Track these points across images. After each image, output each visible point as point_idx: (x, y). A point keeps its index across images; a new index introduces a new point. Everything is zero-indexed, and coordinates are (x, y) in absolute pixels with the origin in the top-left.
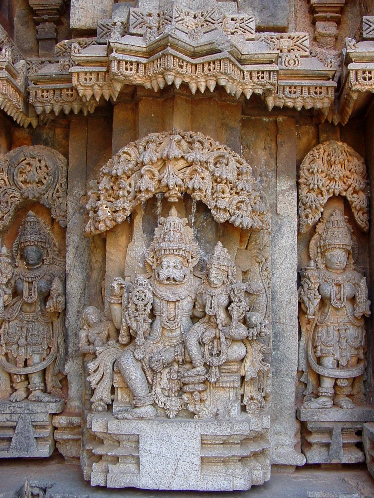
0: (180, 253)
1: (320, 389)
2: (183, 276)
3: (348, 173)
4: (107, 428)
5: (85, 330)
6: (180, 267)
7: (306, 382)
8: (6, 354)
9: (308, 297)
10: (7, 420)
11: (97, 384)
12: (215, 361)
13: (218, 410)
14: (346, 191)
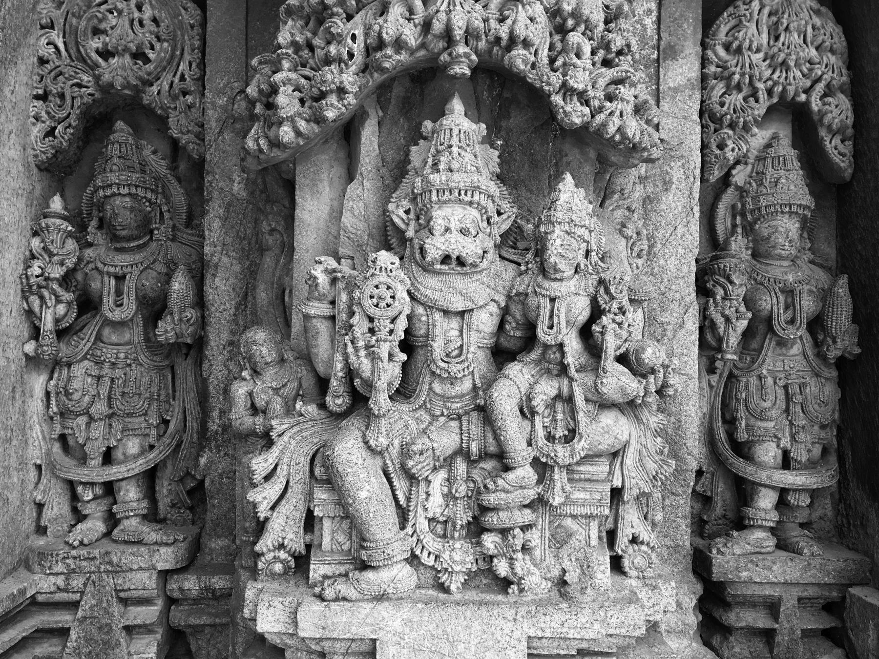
0: (476, 198)
1: (750, 511)
2: (481, 252)
3: (813, 52)
4: (295, 623)
5: (244, 379)
6: (474, 232)
7: (709, 494)
8: (63, 438)
9: (723, 315)
10: (58, 588)
11: (273, 508)
12: (561, 453)
13: (564, 571)
14: (807, 91)
